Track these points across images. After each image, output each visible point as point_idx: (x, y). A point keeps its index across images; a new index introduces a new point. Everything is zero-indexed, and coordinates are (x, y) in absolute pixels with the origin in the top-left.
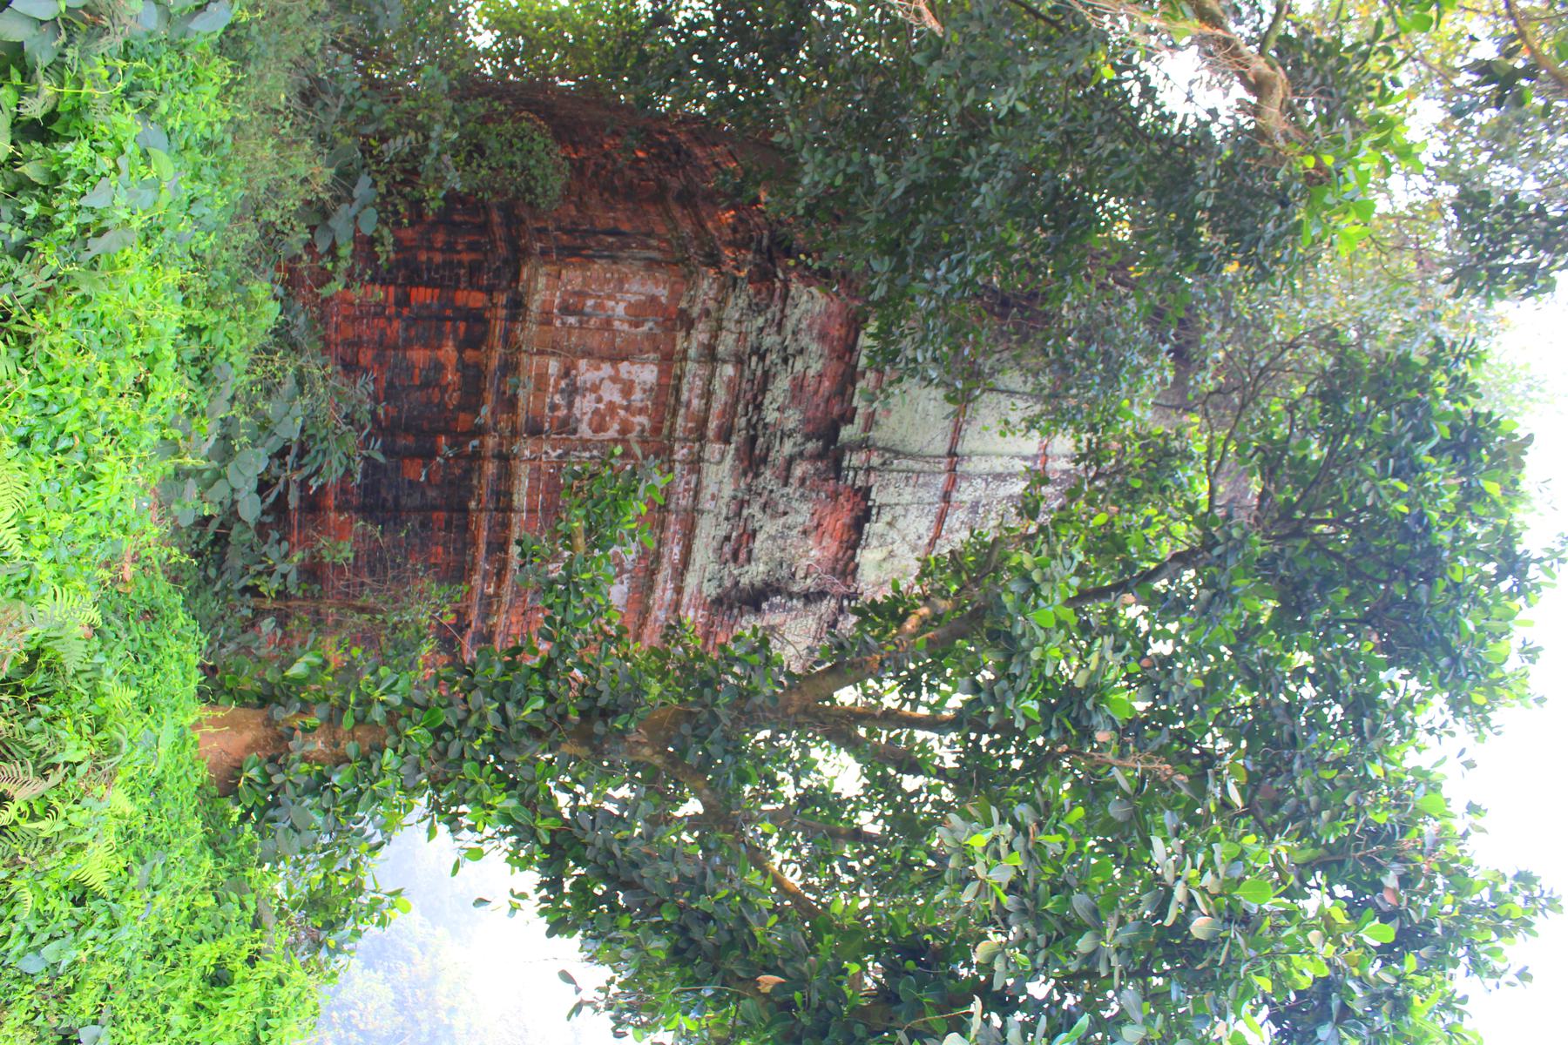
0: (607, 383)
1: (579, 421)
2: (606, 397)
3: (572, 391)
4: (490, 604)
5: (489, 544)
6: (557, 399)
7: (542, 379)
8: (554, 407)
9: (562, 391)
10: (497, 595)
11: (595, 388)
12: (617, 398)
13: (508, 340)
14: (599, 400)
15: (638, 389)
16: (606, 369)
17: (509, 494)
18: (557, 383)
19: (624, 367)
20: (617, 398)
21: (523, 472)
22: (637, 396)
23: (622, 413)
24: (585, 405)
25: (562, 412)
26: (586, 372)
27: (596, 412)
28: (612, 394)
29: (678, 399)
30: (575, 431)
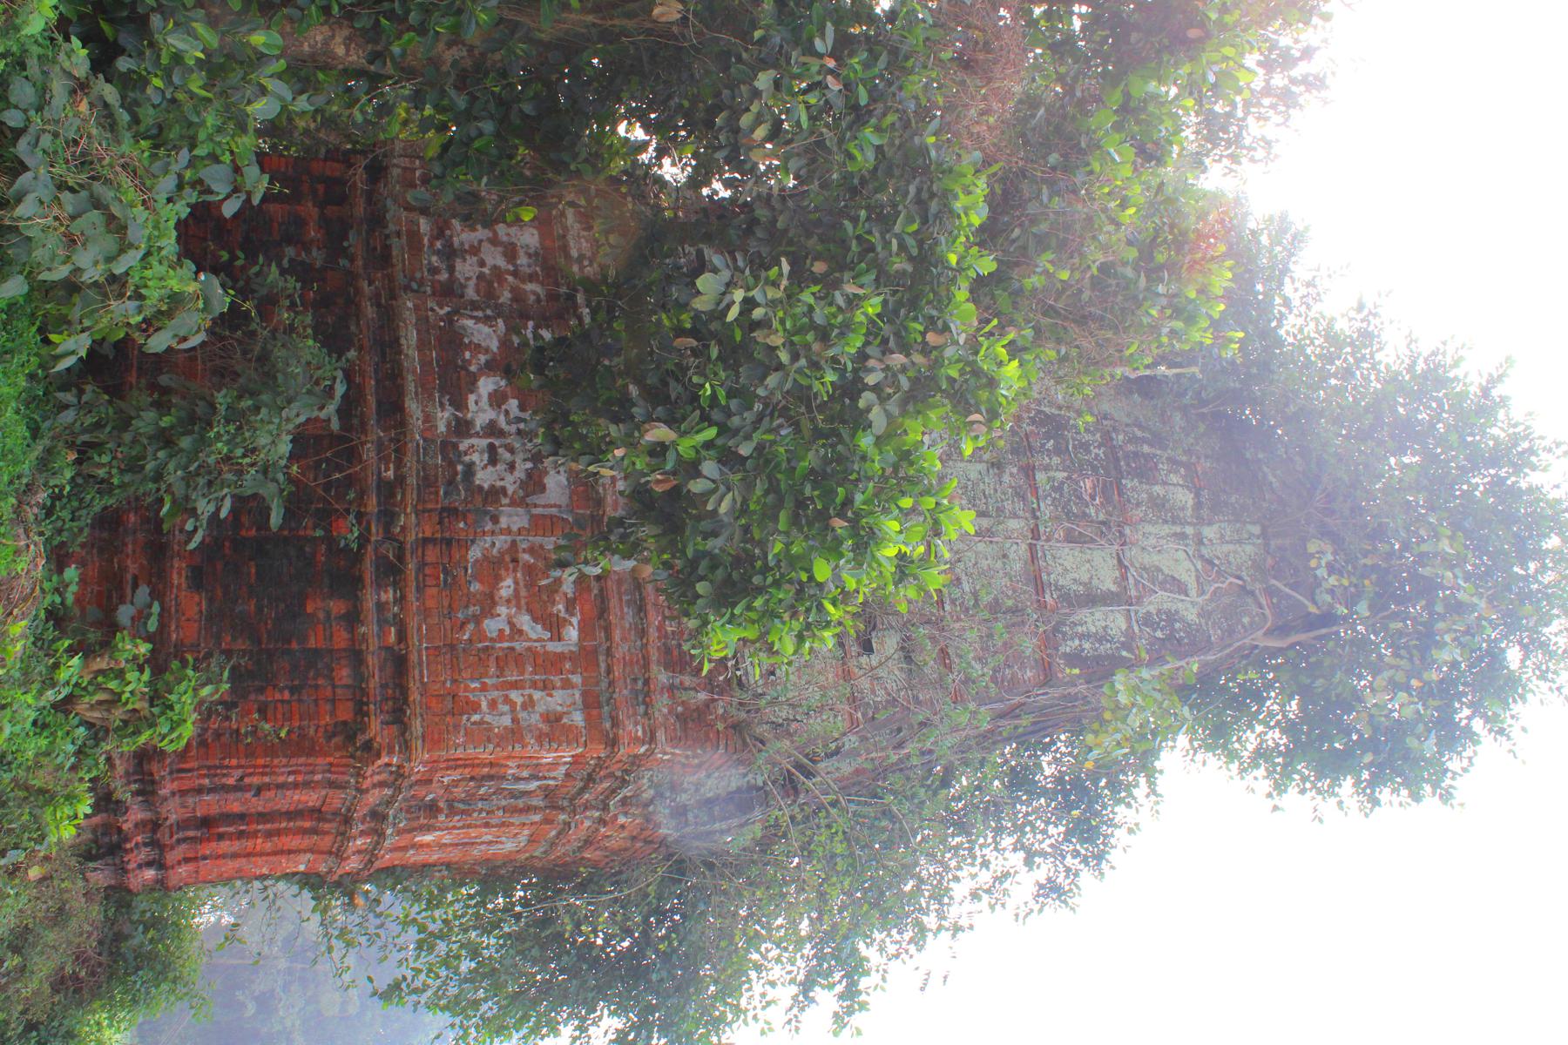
0: (486, 246)
1: (463, 287)
2: (490, 261)
3: (451, 254)
4: (393, 495)
5: (379, 403)
6: (434, 258)
7: (414, 236)
8: (434, 271)
9: (438, 253)
10: (400, 480)
11: (475, 250)
12: (501, 262)
13: (370, 197)
14: (482, 264)
15: (521, 253)
16: (482, 233)
17: (396, 341)
18: (432, 245)
19: (501, 229)
20: (501, 262)
21: (410, 338)
22: (523, 260)
23: (510, 278)
24: (466, 269)
25: (444, 276)
26: (463, 236)
27: (481, 277)
28: (494, 258)
29: (568, 256)
30: (462, 296)
